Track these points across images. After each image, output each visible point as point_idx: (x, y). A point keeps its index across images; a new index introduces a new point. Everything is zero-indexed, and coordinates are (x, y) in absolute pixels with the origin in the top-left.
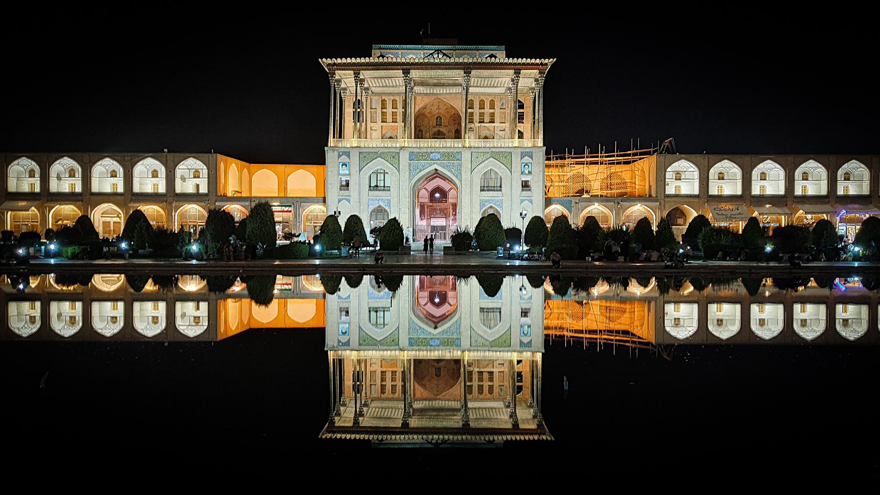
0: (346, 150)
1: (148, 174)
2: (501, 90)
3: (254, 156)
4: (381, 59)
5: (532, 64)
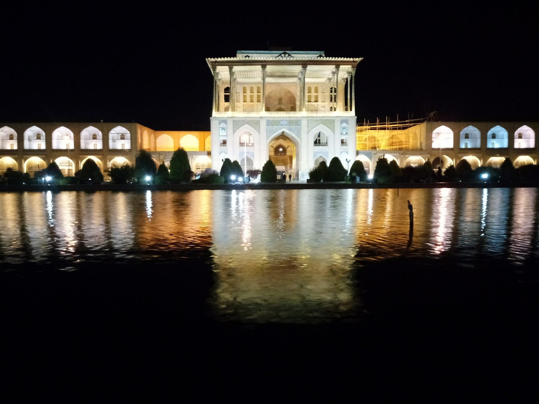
0: (224, 119)
1: (91, 137)
2: (323, 80)
3: (160, 125)
4: (247, 59)
5: (348, 62)
